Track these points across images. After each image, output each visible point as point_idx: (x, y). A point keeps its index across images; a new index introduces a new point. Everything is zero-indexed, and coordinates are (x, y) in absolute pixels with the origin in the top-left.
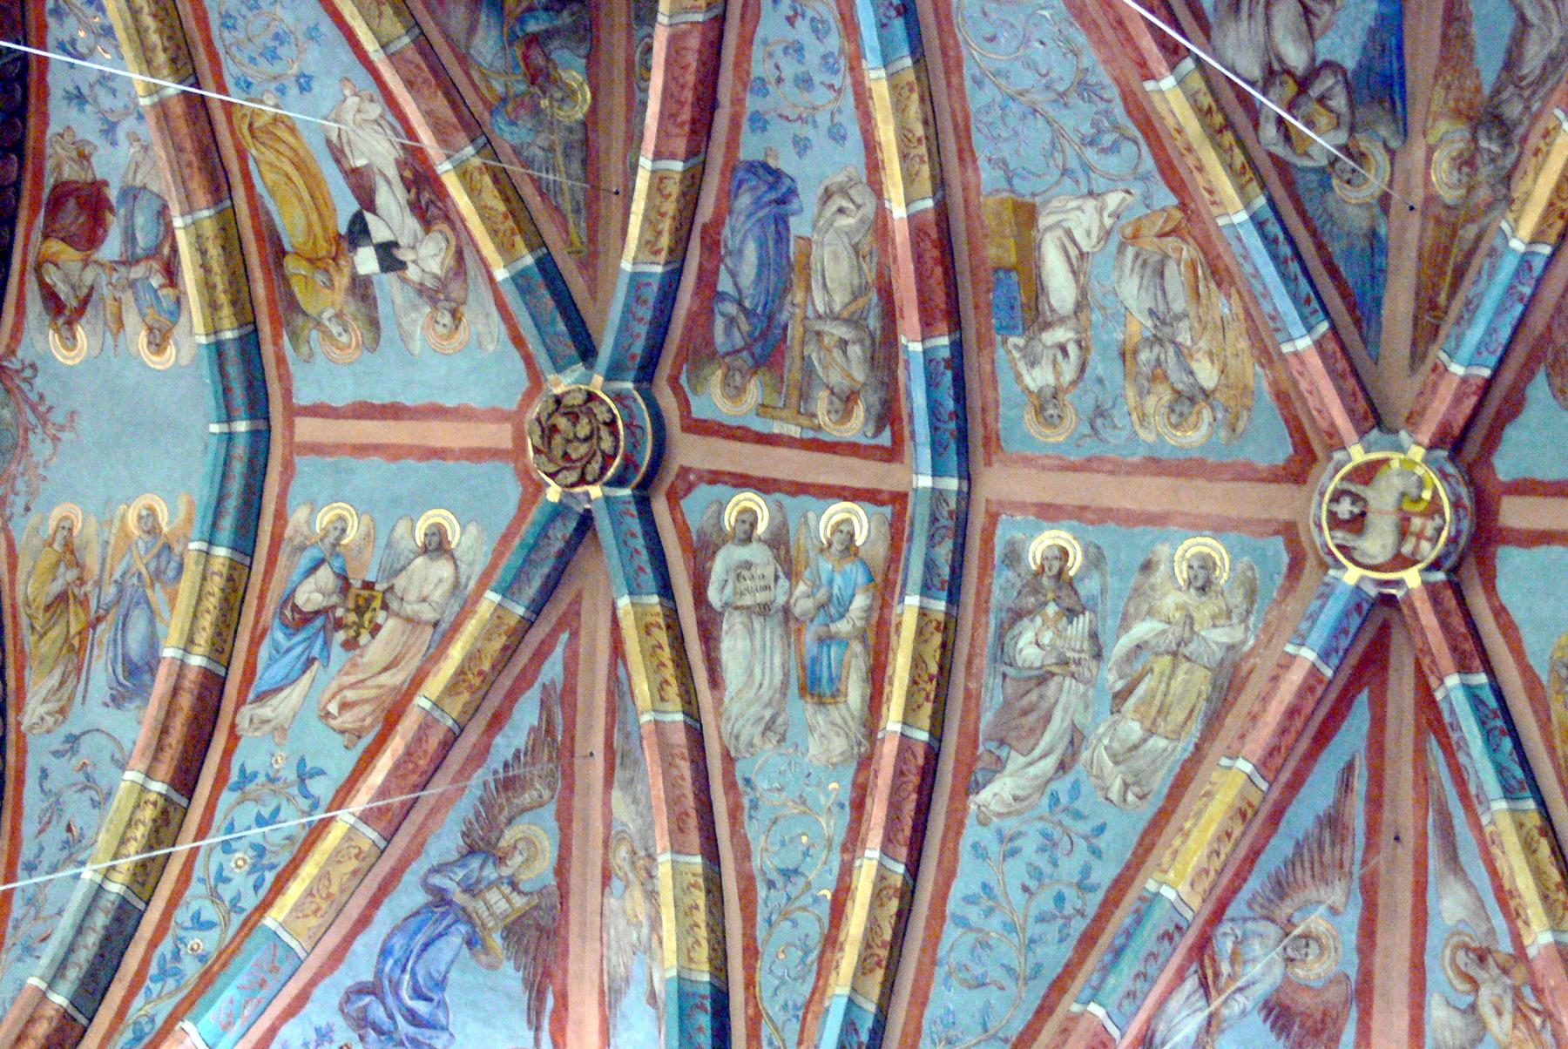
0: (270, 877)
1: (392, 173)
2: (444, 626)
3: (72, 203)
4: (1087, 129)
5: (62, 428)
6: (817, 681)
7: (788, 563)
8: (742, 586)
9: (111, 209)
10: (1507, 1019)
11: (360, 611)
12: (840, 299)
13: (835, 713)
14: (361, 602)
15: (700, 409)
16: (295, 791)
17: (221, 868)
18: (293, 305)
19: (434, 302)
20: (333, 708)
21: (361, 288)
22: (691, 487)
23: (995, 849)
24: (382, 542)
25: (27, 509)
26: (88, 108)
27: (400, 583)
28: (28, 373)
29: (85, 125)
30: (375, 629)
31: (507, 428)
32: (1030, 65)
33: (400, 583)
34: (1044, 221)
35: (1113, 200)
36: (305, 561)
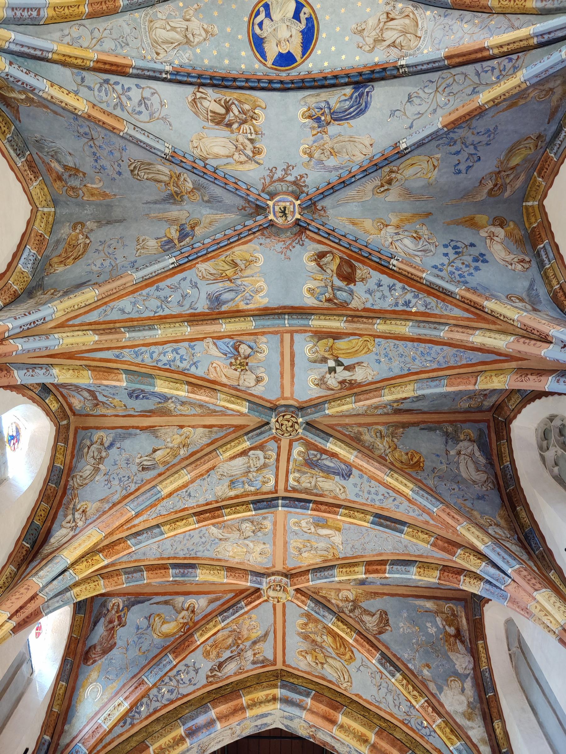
0: (168, 367)
1: (353, 378)
2: (238, 387)
3: (350, 270)
4: (356, 547)
5: (285, 255)
6: (234, 483)
7: (259, 469)
8: (254, 459)
9: (348, 284)
10: (182, 621)
11: (240, 364)
12: (320, 484)
13: (227, 490)
14: (242, 364)
15: (295, 444)
16: (191, 362)
17: (167, 352)
18: (320, 339)
19: (321, 380)
20: (214, 365)
21: (324, 360)
22: (276, 442)
23: (201, 534)
24: (259, 365)
25: (261, 244)
26: (376, 287)
27: (249, 372)
28: (301, 242)
29: (371, 284)
30: (236, 370)
31: (290, 396)
32: (369, 542)
33: (249, 372)
34: (337, 532)
35: (341, 547)
36: (252, 344)
